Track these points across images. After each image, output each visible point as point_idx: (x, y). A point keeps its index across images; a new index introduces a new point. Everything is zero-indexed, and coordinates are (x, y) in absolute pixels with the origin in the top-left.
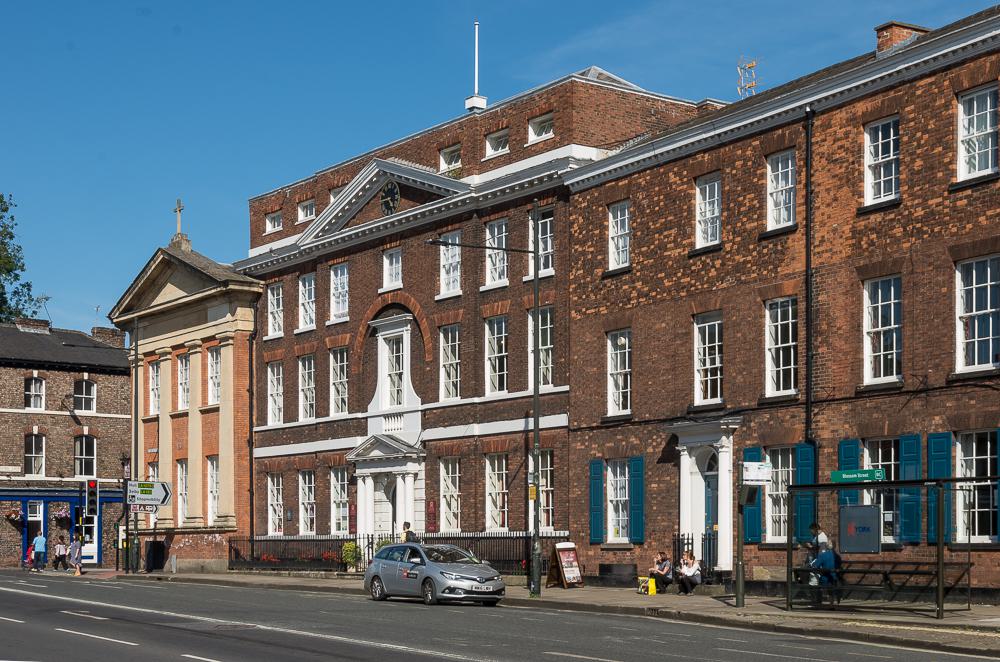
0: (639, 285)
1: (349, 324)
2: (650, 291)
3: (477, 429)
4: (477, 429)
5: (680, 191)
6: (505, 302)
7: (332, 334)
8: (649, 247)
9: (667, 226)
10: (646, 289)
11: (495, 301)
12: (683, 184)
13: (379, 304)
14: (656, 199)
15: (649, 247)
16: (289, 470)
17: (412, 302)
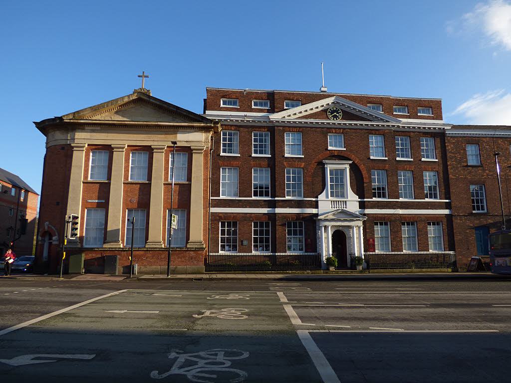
1: (303, 159)
3: (400, 211)
4: (400, 211)
16: (245, 220)
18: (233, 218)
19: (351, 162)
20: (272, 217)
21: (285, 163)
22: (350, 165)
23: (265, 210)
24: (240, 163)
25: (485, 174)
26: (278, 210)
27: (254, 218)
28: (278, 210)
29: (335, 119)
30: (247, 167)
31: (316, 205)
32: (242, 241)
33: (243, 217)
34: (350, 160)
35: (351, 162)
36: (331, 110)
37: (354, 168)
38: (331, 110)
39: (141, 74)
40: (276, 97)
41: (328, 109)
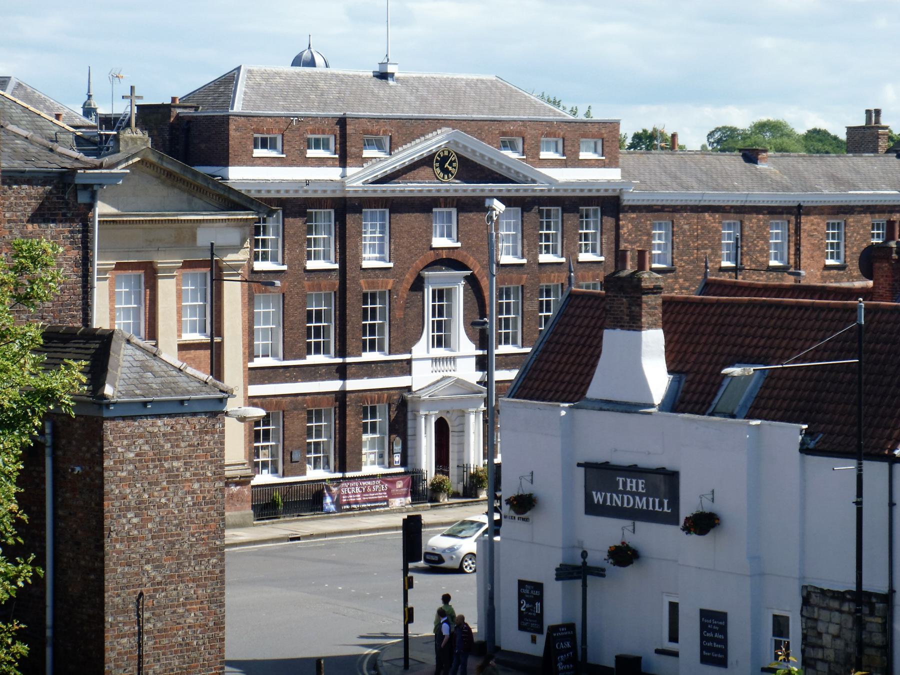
0: (681, 280)
1: (391, 270)
2: (689, 286)
5: (713, 227)
6: (561, 274)
7: (370, 277)
8: (689, 257)
9: (704, 247)
10: (687, 284)
11: (552, 272)
12: (715, 222)
13: (431, 257)
14: (695, 227)
15: (689, 257)
16: (295, 409)
17: (470, 261)
18: (276, 404)
19: (468, 273)
20: (342, 395)
21: (362, 281)
22: (466, 278)
23: (334, 385)
24: (287, 284)
25: (677, 286)
26: (353, 385)
27: (310, 404)
28: (353, 385)
29: (446, 177)
30: (297, 294)
31: (406, 368)
32: (291, 453)
33: (291, 402)
34: (464, 267)
35: (468, 273)
36: (439, 156)
37: (473, 283)
38: (439, 156)
39: (137, 93)
40: (350, 129)
41: (435, 154)
